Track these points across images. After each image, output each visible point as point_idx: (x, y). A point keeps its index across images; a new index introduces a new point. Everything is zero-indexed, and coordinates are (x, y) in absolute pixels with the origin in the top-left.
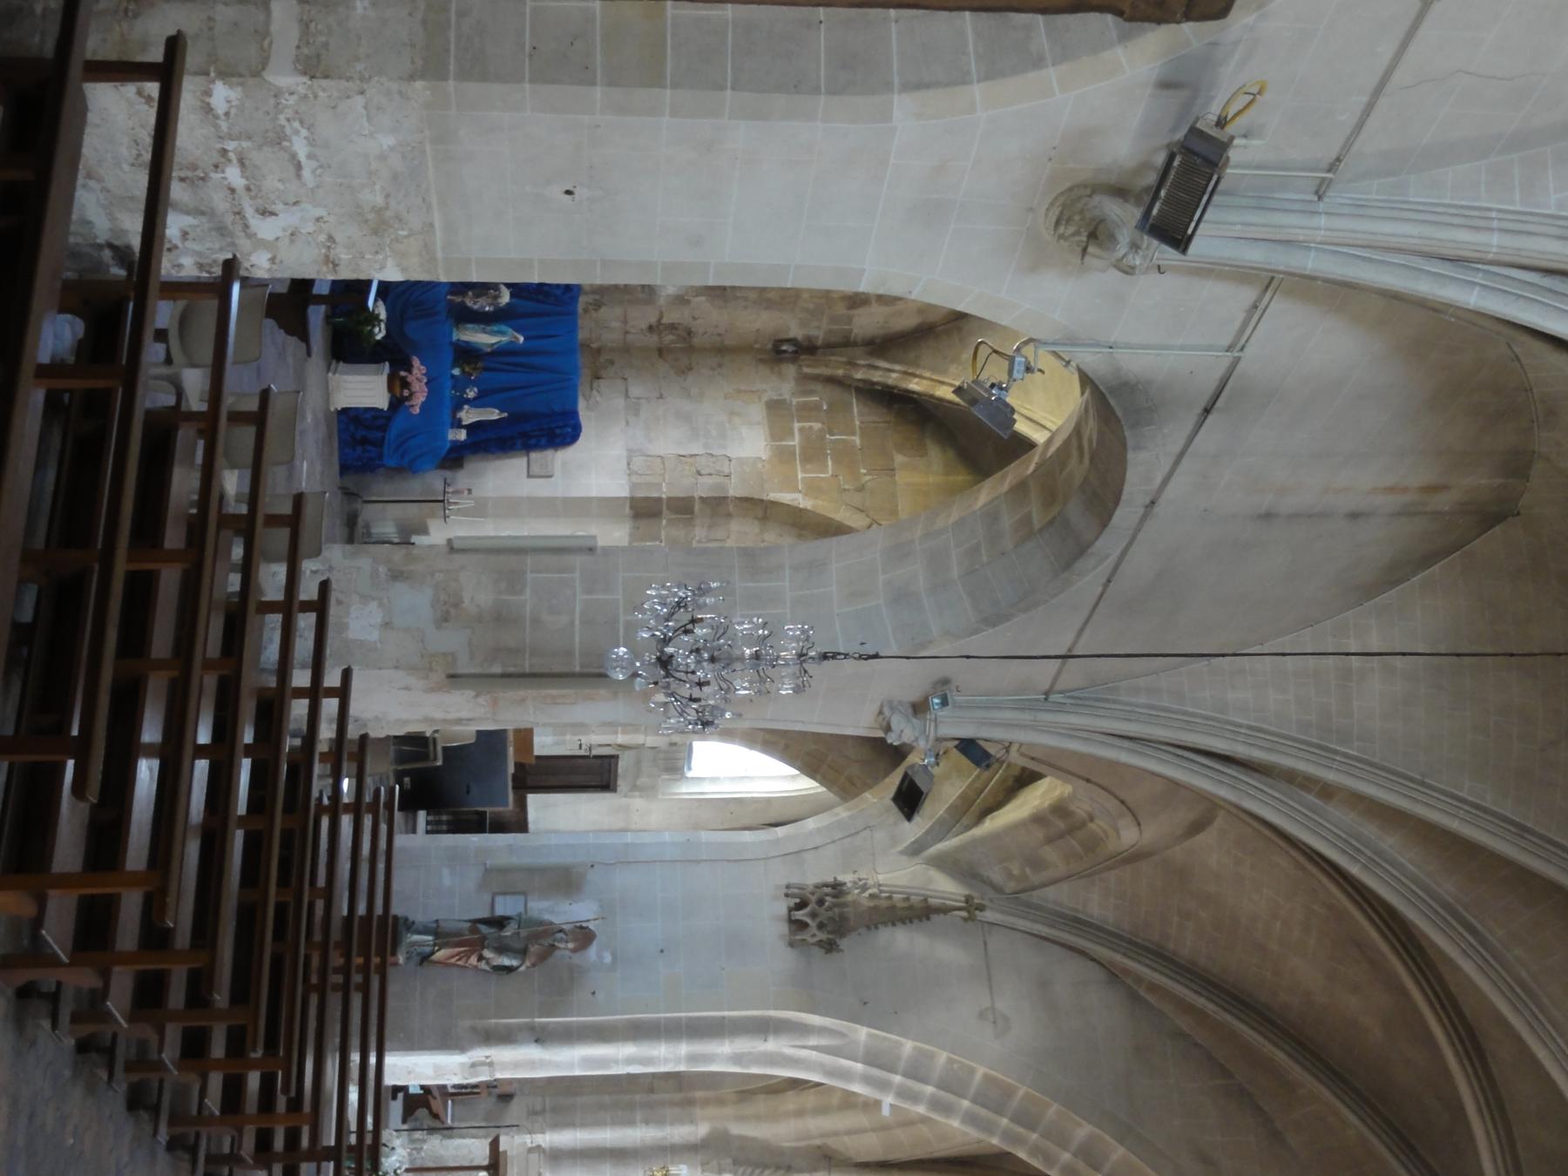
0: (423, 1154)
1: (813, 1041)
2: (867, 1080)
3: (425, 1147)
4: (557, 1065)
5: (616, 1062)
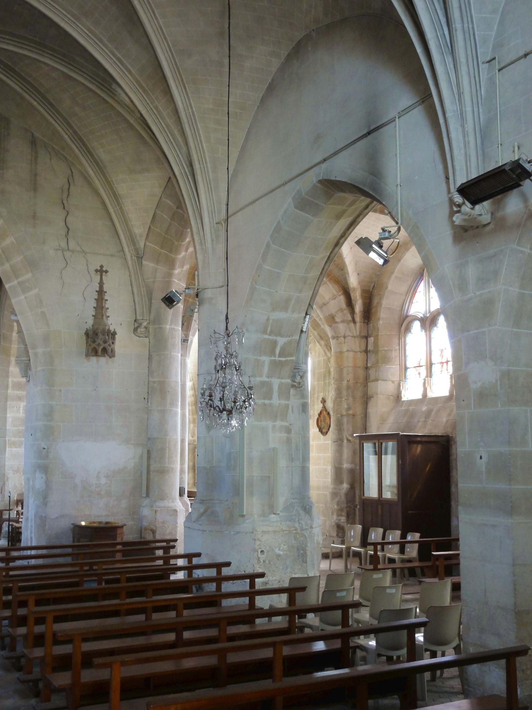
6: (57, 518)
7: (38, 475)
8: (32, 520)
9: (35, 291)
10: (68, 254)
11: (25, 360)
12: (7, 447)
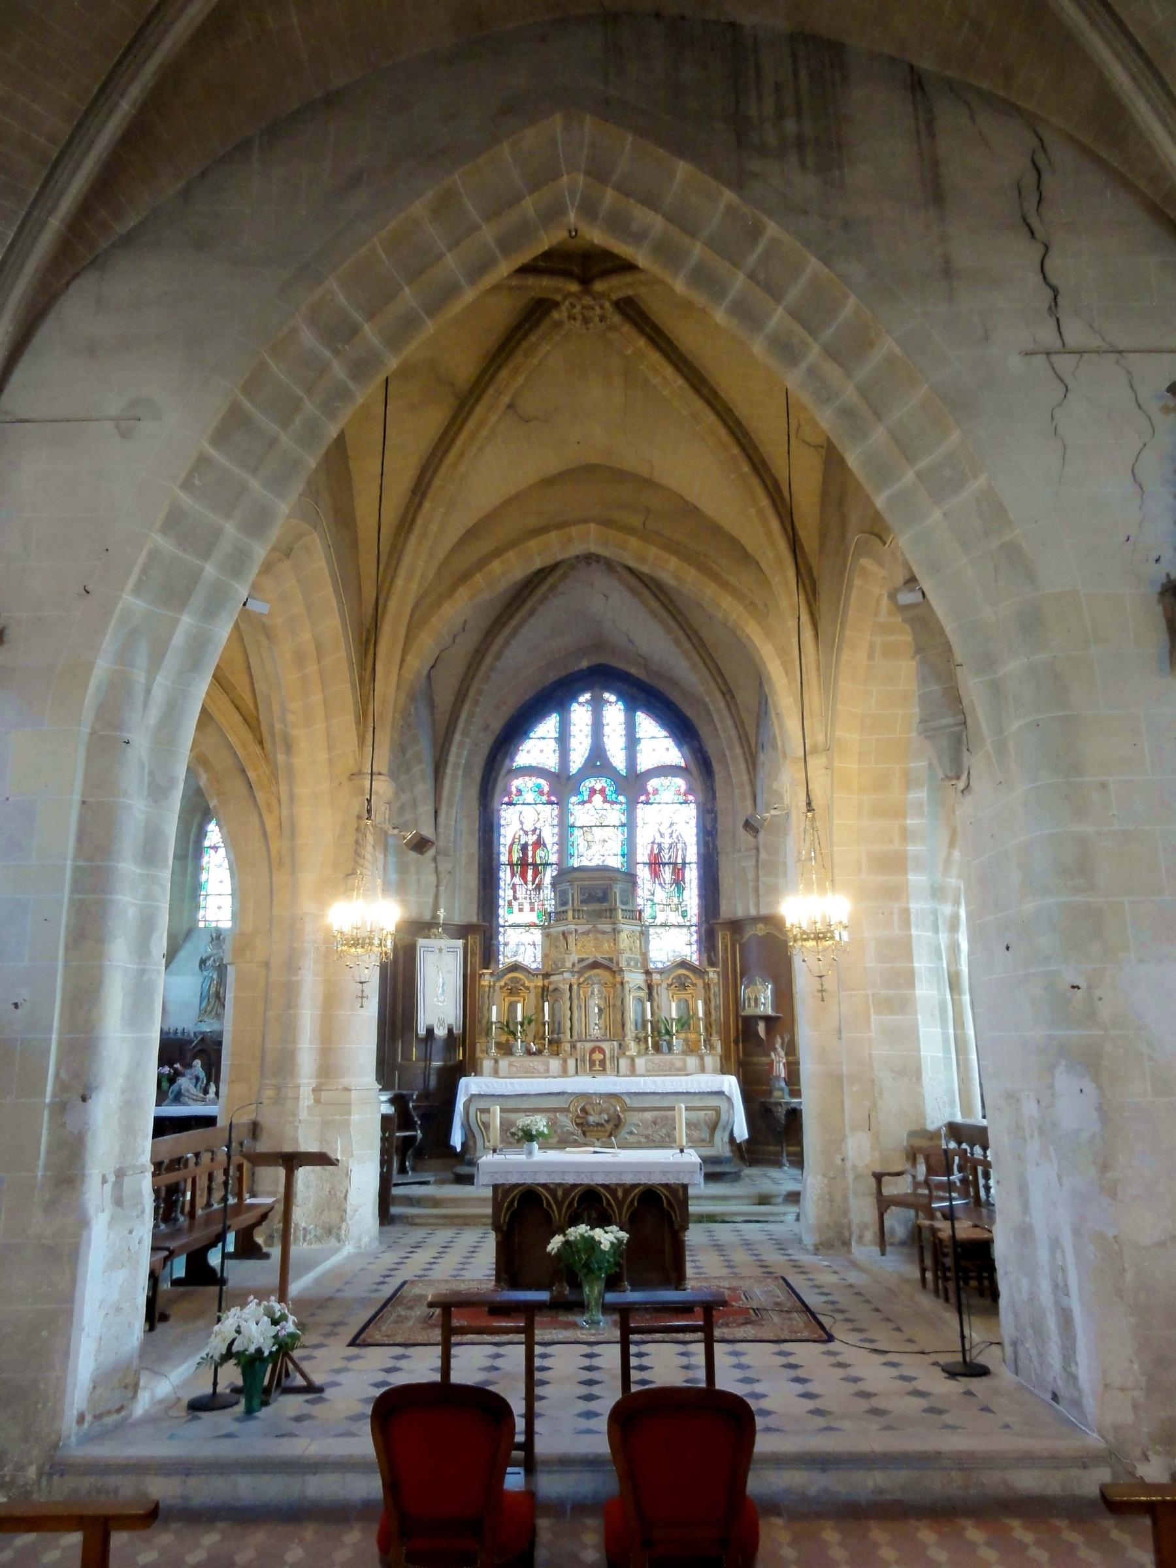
0: (312, 1227)
1: (140, 677)
2: (210, 612)
3: (303, 1225)
4: (137, 1065)
5: (142, 972)
6: (1161, 1244)
7: (1065, 1082)
8: (1055, 1244)
9: (980, 482)
10: (1064, 363)
11: (949, 726)
12: (872, 1010)
